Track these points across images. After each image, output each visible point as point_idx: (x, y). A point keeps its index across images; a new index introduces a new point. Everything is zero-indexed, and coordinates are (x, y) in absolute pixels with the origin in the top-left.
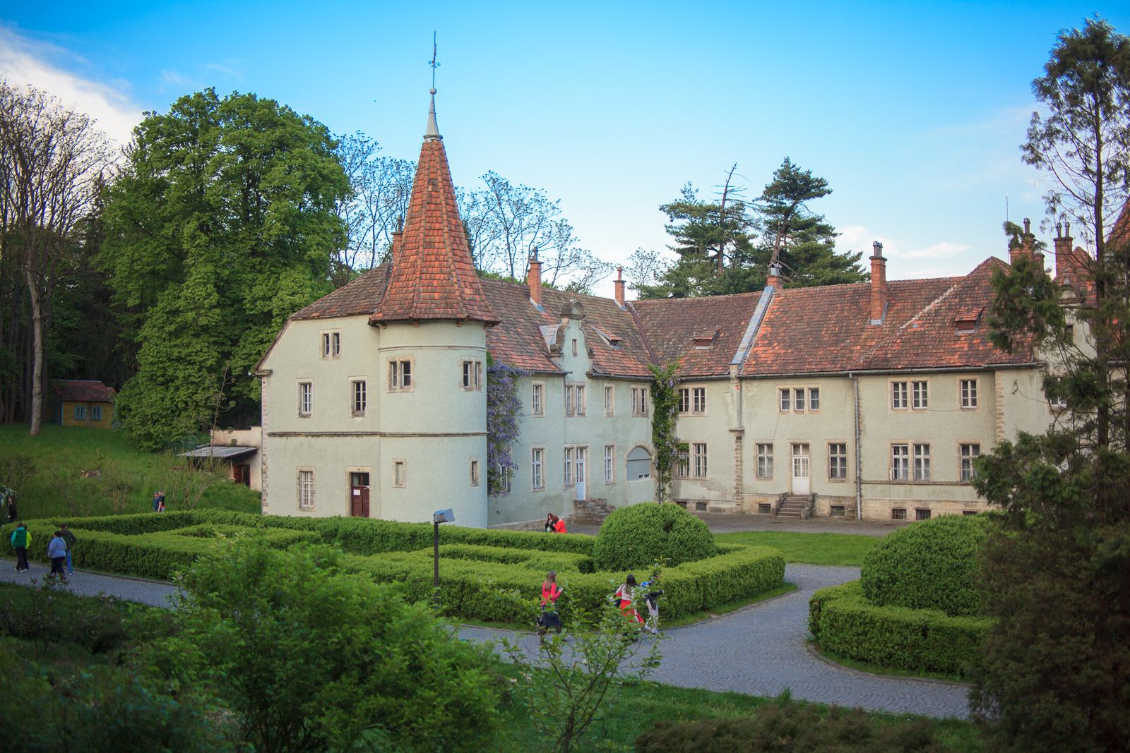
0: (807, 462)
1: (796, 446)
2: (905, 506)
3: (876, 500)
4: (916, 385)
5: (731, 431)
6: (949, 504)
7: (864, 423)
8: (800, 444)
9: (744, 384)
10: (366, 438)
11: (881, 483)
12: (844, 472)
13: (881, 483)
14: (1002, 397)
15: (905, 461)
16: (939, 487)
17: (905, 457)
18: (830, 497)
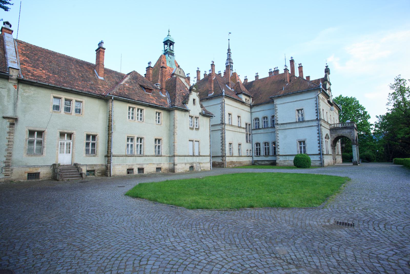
0: (70, 145)
1: (62, 134)
2: (133, 167)
3: (120, 165)
4: (138, 110)
5: (4, 118)
6: (151, 165)
7: (115, 124)
8: (66, 133)
9: (21, 86)
11: (122, 156)
12: (94, 152)
13: (122, 156)
14: (177, 120)
15: (132, 145)
16: (147, 157)
17: (132, 143)
18: (87, 165)
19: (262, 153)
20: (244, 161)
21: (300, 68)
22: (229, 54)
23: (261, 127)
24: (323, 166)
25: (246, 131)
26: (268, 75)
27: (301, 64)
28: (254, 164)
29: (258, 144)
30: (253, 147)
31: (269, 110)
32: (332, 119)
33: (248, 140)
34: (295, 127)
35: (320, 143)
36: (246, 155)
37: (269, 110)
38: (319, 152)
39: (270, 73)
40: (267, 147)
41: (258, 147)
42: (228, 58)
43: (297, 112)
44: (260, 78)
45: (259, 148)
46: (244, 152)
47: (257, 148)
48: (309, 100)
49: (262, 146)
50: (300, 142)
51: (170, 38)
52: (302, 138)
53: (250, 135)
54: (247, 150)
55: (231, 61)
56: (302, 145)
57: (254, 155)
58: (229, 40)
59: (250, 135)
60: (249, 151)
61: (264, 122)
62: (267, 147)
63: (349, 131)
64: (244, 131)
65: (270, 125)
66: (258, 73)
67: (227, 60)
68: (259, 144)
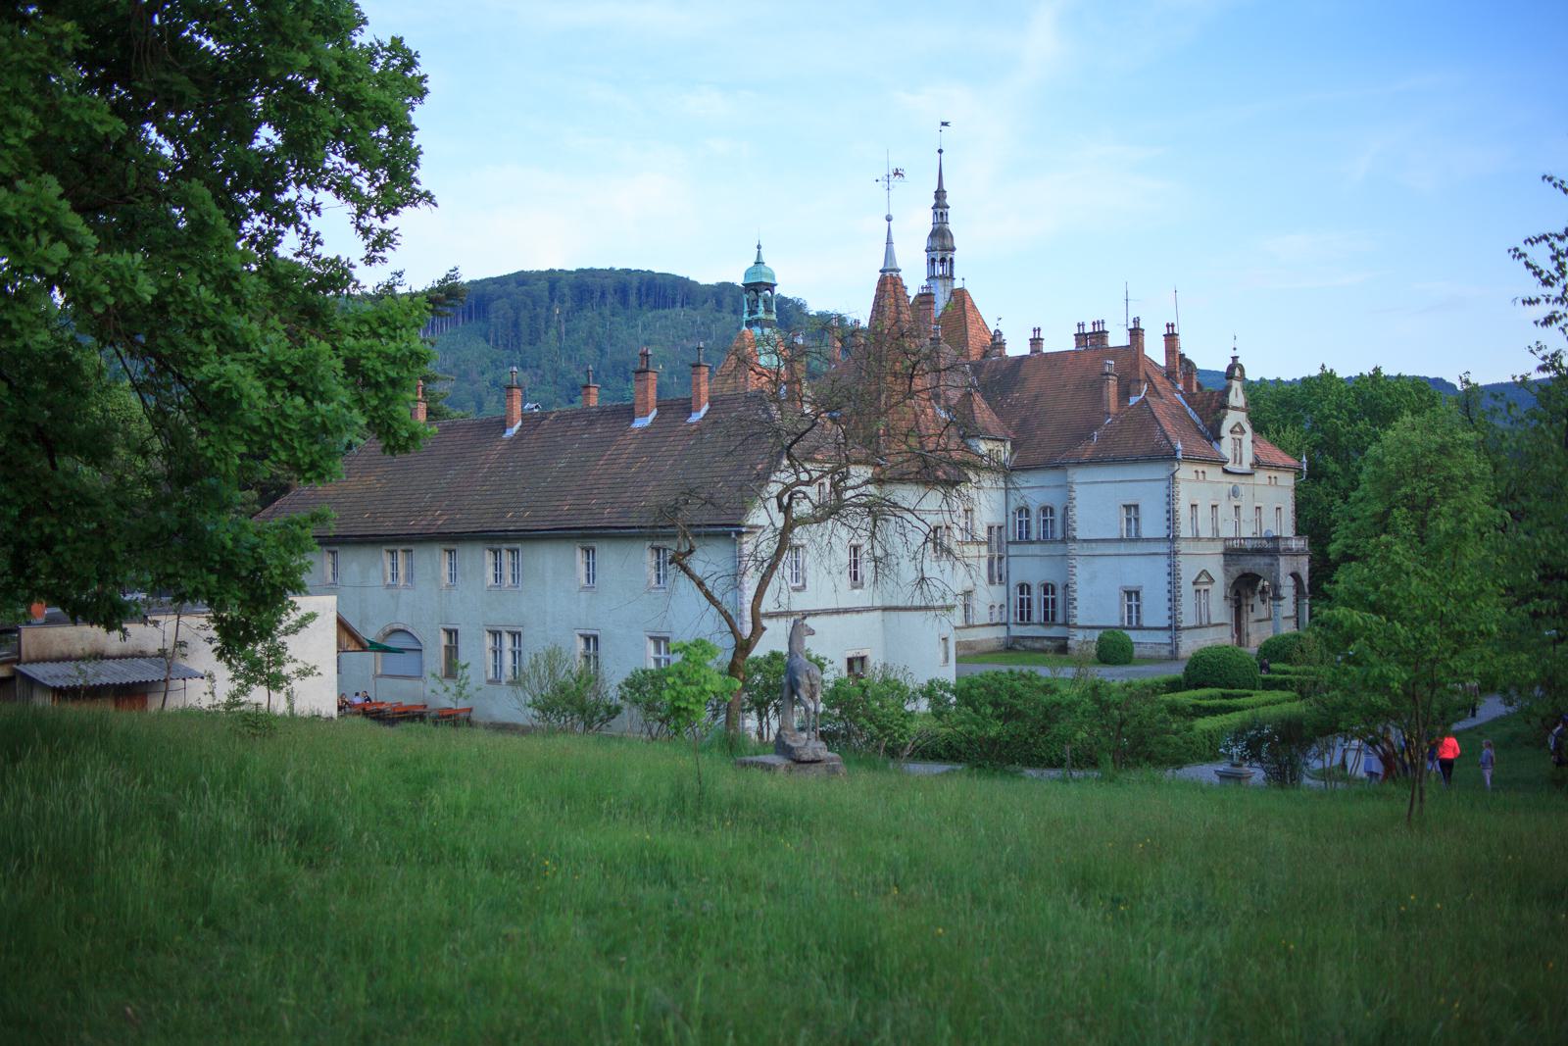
10: (865, 614)
19: (1037, 614)
20: (982, 641)
21: (1171, 338)
22: (939, 211)
23: (1034, 536)
24: (1177, 659)
25: (990, 550)
26: (1071, 345)
27: (1173, 326)
28: (1011, 647)
29: (1024, 588)
30: (1011, 595)
31: (1057, 486)
32: (1247, 513)
33: (996, 576)
34: (1117, 552)
35: (1174, 598)
36: (988, 621)
37: (1057, 486)
38: (1169, 622)
39: (1080, 337)
40: (1050, 597)
41: (1026, 596)
42: (937, 226)
43: (1124, 511)
44: (1047, 348)
45: (1029, 600)
46: (981, 613)
47: (1022, 600)
48: (1153, 484)
49: (1037, 596)
50: (1129, 593)
51: (766, 275)
52: (1132, 584)
53: (1000, 558)
54: (992, 607)
55: (947, 243)
56: (1134, 603)
57: (1012, 621)
58: (940, 151)
59: (1000, 558)
60: (996, 609)
61: (1045, 521)
62: (1050, 597)
63: (1267, 560)
64: (984, 550)
65: (1059, 535)
66: (1039, 330)
67: (933, 235)
68: (1029, 587)
